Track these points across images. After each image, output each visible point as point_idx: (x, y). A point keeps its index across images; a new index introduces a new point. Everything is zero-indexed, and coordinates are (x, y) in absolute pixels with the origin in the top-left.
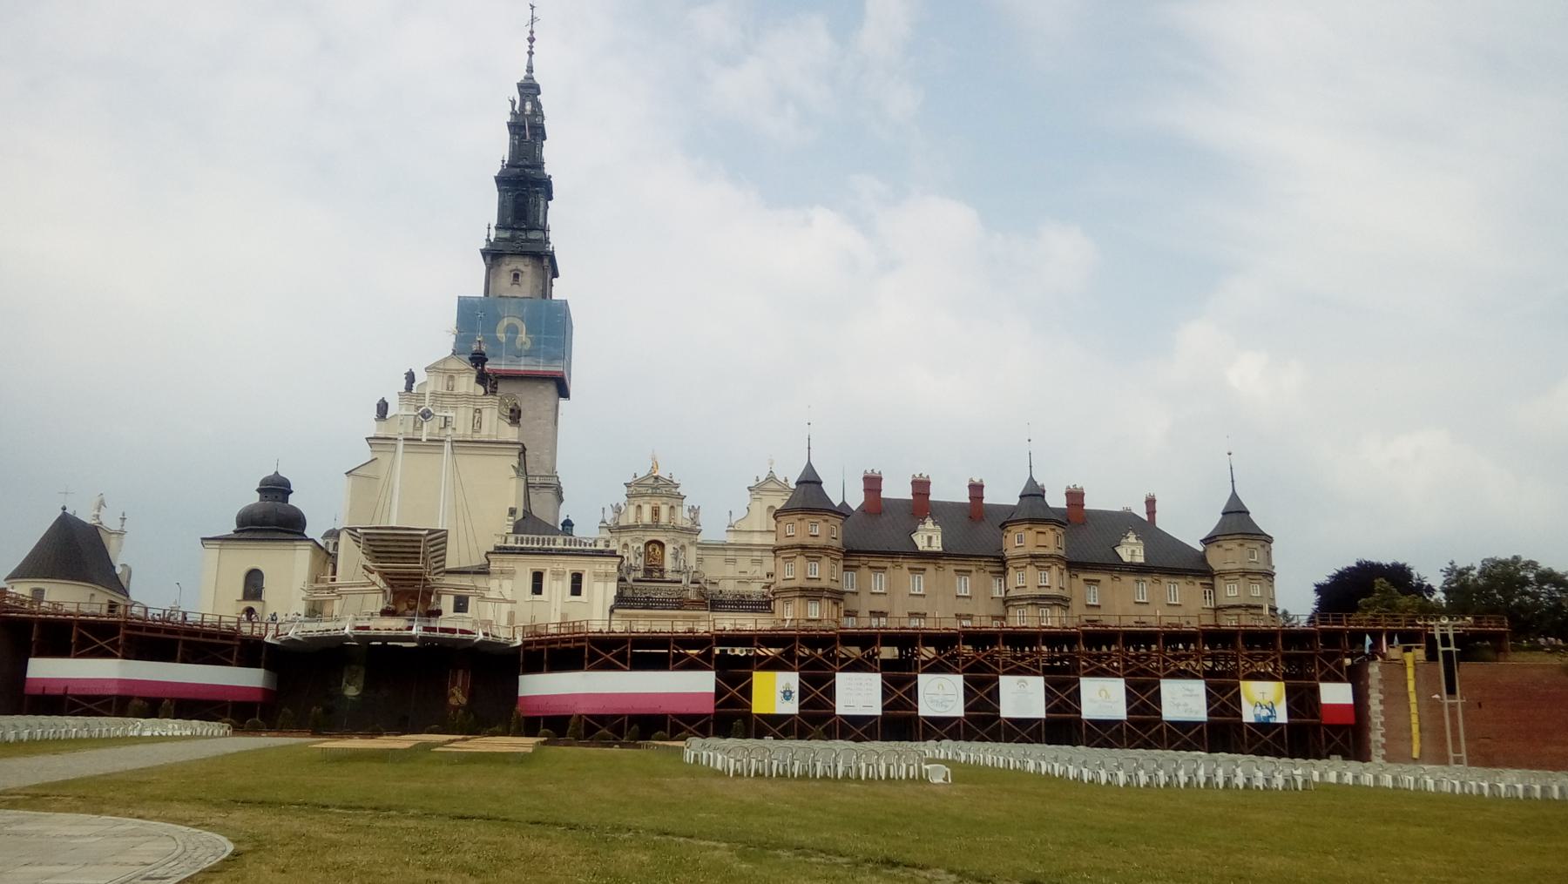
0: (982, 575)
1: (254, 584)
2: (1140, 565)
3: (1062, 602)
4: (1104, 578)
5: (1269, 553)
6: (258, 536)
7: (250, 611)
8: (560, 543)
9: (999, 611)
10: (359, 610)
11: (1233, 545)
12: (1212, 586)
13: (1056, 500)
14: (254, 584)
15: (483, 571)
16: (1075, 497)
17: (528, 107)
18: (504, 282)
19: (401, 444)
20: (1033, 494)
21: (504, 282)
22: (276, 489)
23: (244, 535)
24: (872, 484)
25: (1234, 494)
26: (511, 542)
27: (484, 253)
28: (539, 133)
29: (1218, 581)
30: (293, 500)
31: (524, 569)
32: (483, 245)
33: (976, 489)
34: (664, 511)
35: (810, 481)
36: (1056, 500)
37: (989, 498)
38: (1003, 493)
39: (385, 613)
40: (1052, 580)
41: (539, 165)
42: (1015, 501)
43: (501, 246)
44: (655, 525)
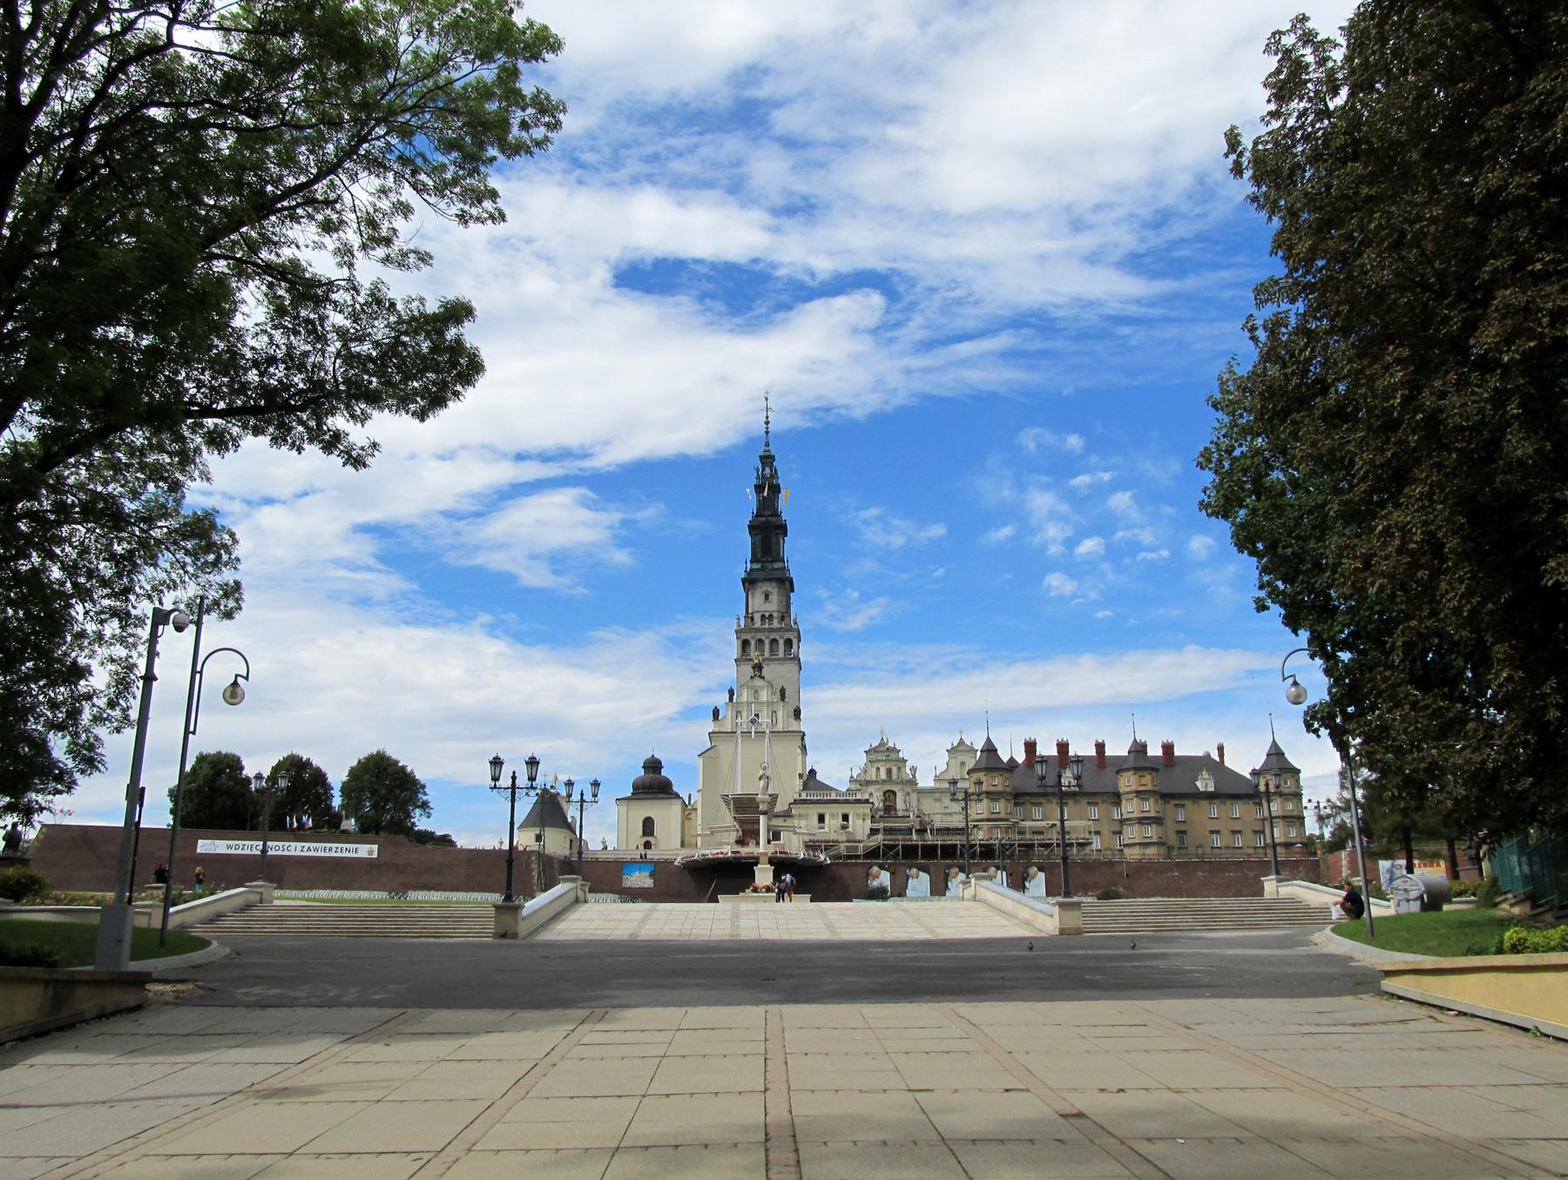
3: (1157, 821)
4: (1188, 803)
5: (1298, 780)
7: (647, 845)
9: (1117, 829)
13: (1155, 751)
15: (787, 815)
17: (768, 470)
18: (757, 602)
20: (1139, 749)
21: (757, 602)
22: (653, 766)
24: (1030, 747)
26: (804, 796)
27: (744, 581)
28: (775, 490)
30: (664, 773)
31: (814, 811)
32: (743, 575)
33: (1100, 747)
34: (894, 770)
35: (990, 749)
36: (1155, 751)
38: (1118, 748)
40: (1150, 807)
41: (777, 514)
43: (755, 575)
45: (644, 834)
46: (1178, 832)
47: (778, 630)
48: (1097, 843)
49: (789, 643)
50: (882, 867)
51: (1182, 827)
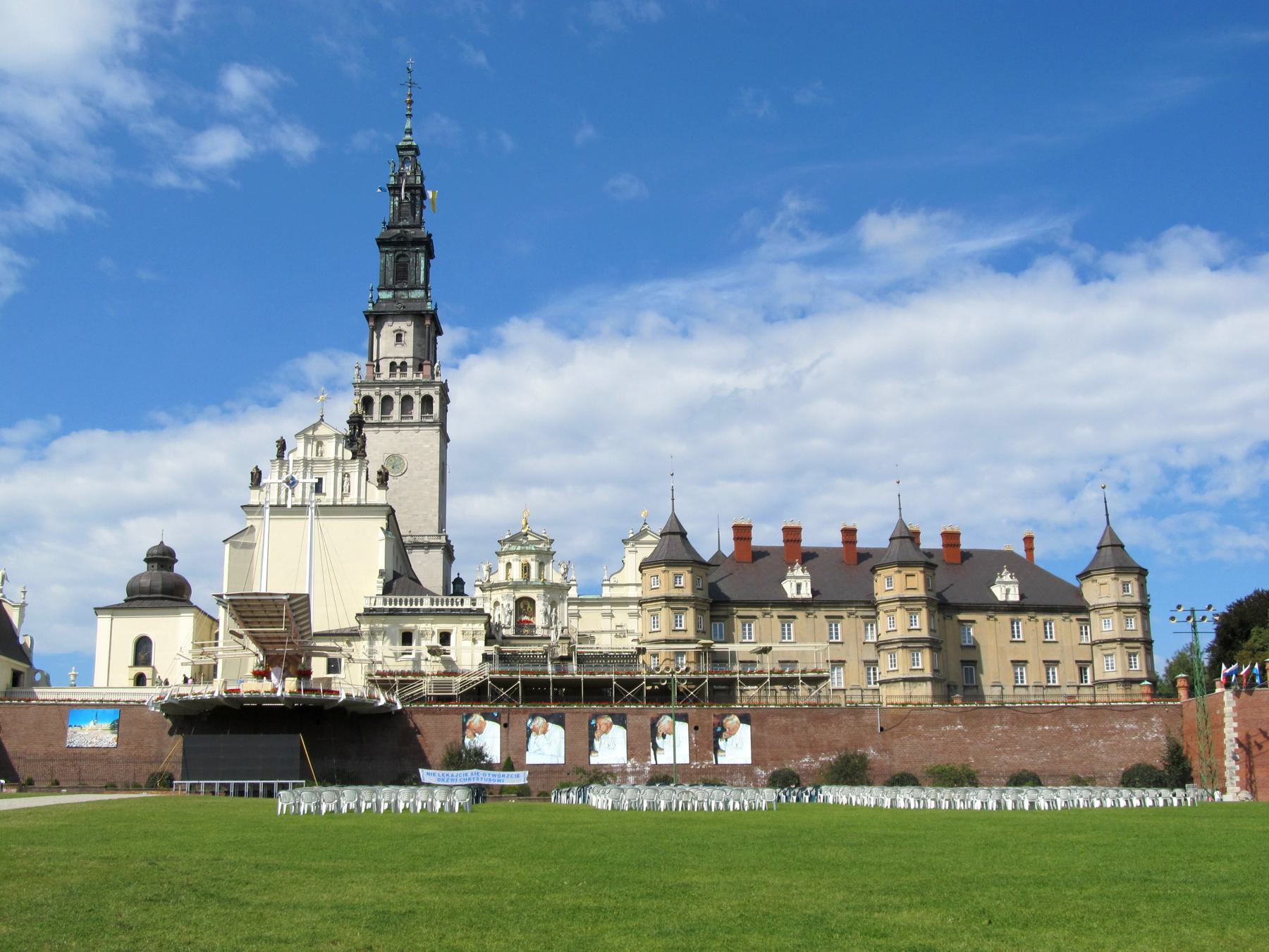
0: (852, 619)
1: (143, 648)
2: (1014, 603)
6: (147, 603)
8: (427, 604)
9: (870, 654)
10: (240, 672)
11: (1107, 579)
12: (1088, 620)
13: (931, 541)
14: (143, 648)
16: (951, 538)
17: (408, 169)
19: (268, 511)
22: (162, 558)
23: (134, 604)
25: (1109, 531)
26: (380, 605)
28: (417, 192)
29: (1092, 614)
30: (178, 569)
33: (849, 534)
35: (675, 532)
37: (862, 543)
39: (261, 675)
42: (884, 543)
44: (526, 583)
45: (137, 663)
46: (964, 662)
47: (412, 384)
48: (838, 679)
49: (427, 401)
50: (487, 716)
51: (969, 656)
